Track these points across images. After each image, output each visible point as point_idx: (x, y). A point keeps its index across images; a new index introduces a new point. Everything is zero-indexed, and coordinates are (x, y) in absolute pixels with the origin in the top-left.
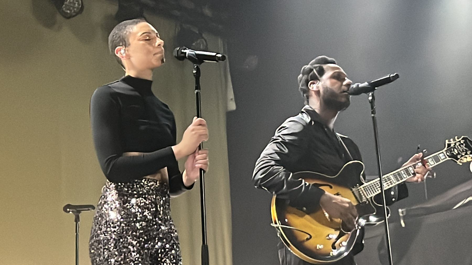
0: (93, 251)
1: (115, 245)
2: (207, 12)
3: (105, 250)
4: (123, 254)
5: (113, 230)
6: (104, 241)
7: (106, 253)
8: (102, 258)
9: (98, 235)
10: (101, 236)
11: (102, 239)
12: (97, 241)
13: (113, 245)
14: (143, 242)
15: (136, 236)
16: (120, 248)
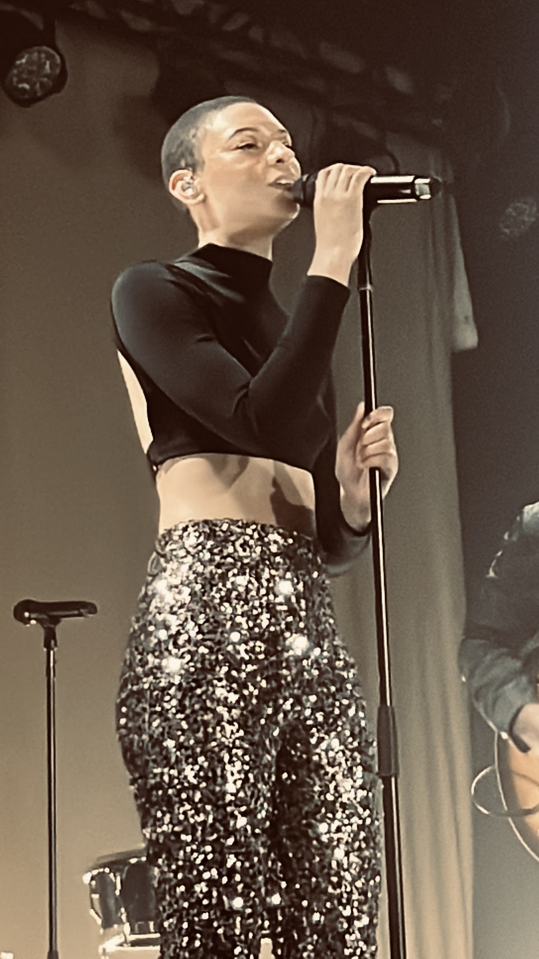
2: (400, 82)
3: (155, 716)
4: (202, 729)
6: (152, 692)
7: (155, 724)
8: (145, 737)
10: (145, 680)
11: (146, 686)
12: (132, 692)
13: (174, 702)
14: (257, 697)
16: (194, 712)
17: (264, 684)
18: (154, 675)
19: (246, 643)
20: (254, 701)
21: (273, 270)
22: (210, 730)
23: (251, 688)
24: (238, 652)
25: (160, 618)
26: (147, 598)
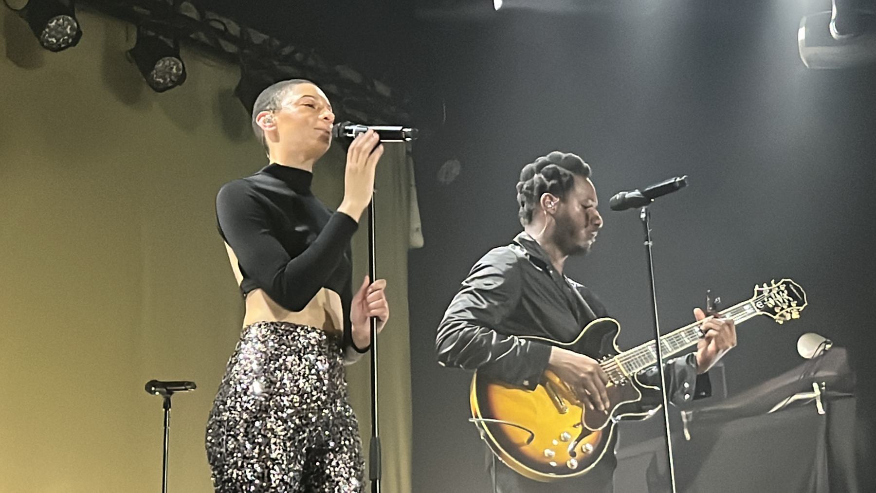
0: (209, 438)
1: (246, 429)
5: (245, 405)
7: (230, 442)
8: (223, 450)
9: (219, 413)
11: (225, 418)
12: (217, 421)
13: (242, 430)
15: (281, 418)
16: (254, 436)
17: (297, 421)
18: (230, 411)
19: (288, 396)
20: (291, 431)
21: (314, 180)
22: (263, 448)
23: (290, 423)
24: (283, 401)
25: (238, 377)
26: (232, 365)
